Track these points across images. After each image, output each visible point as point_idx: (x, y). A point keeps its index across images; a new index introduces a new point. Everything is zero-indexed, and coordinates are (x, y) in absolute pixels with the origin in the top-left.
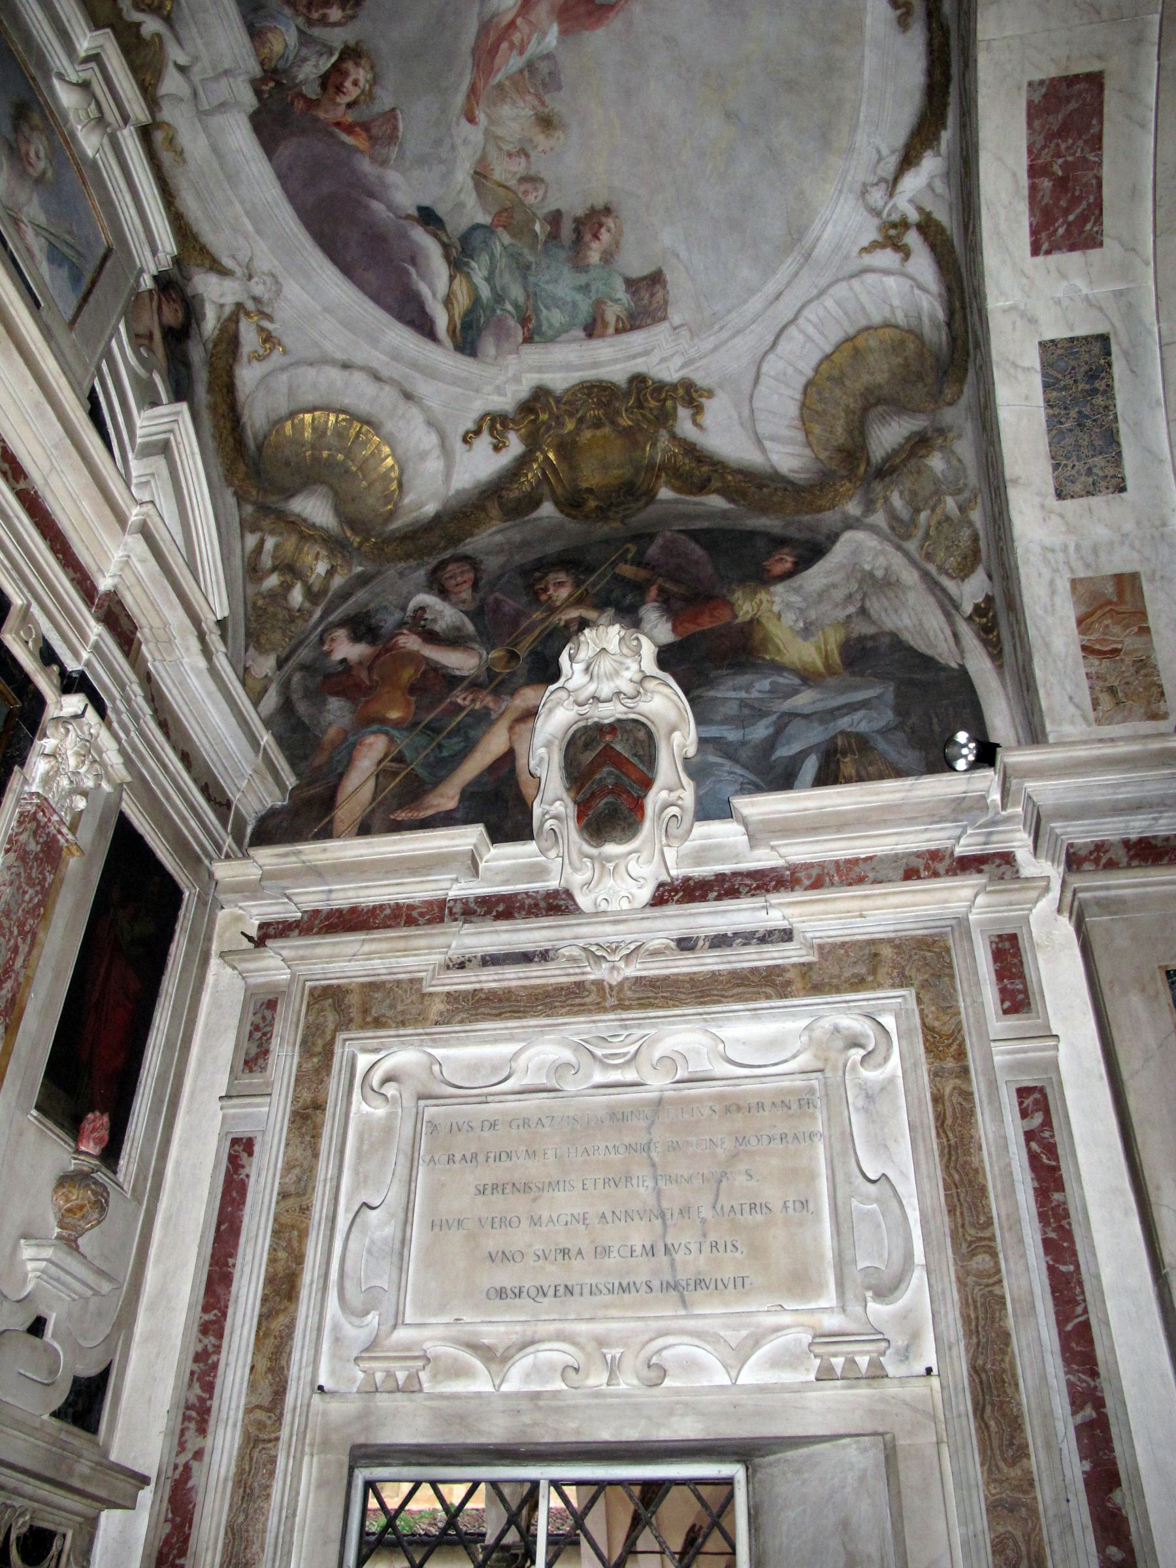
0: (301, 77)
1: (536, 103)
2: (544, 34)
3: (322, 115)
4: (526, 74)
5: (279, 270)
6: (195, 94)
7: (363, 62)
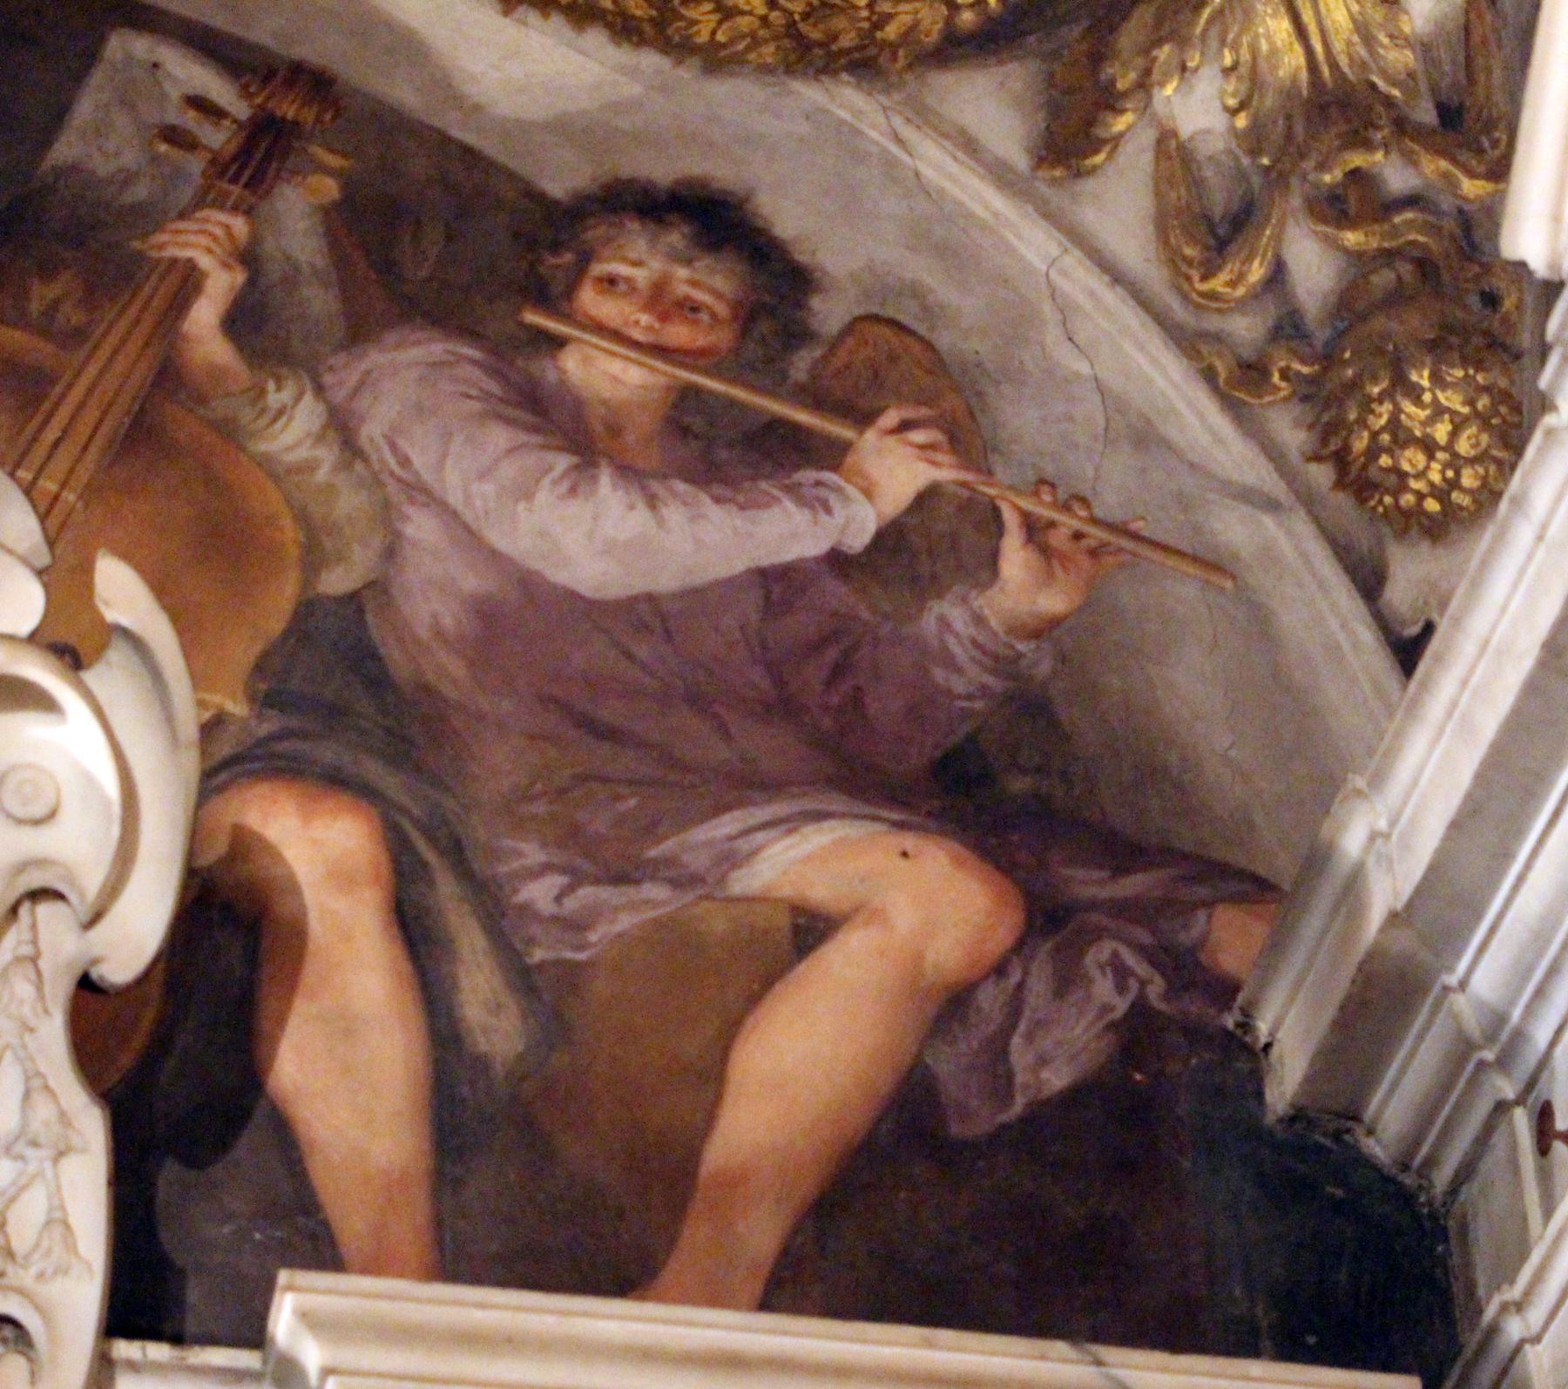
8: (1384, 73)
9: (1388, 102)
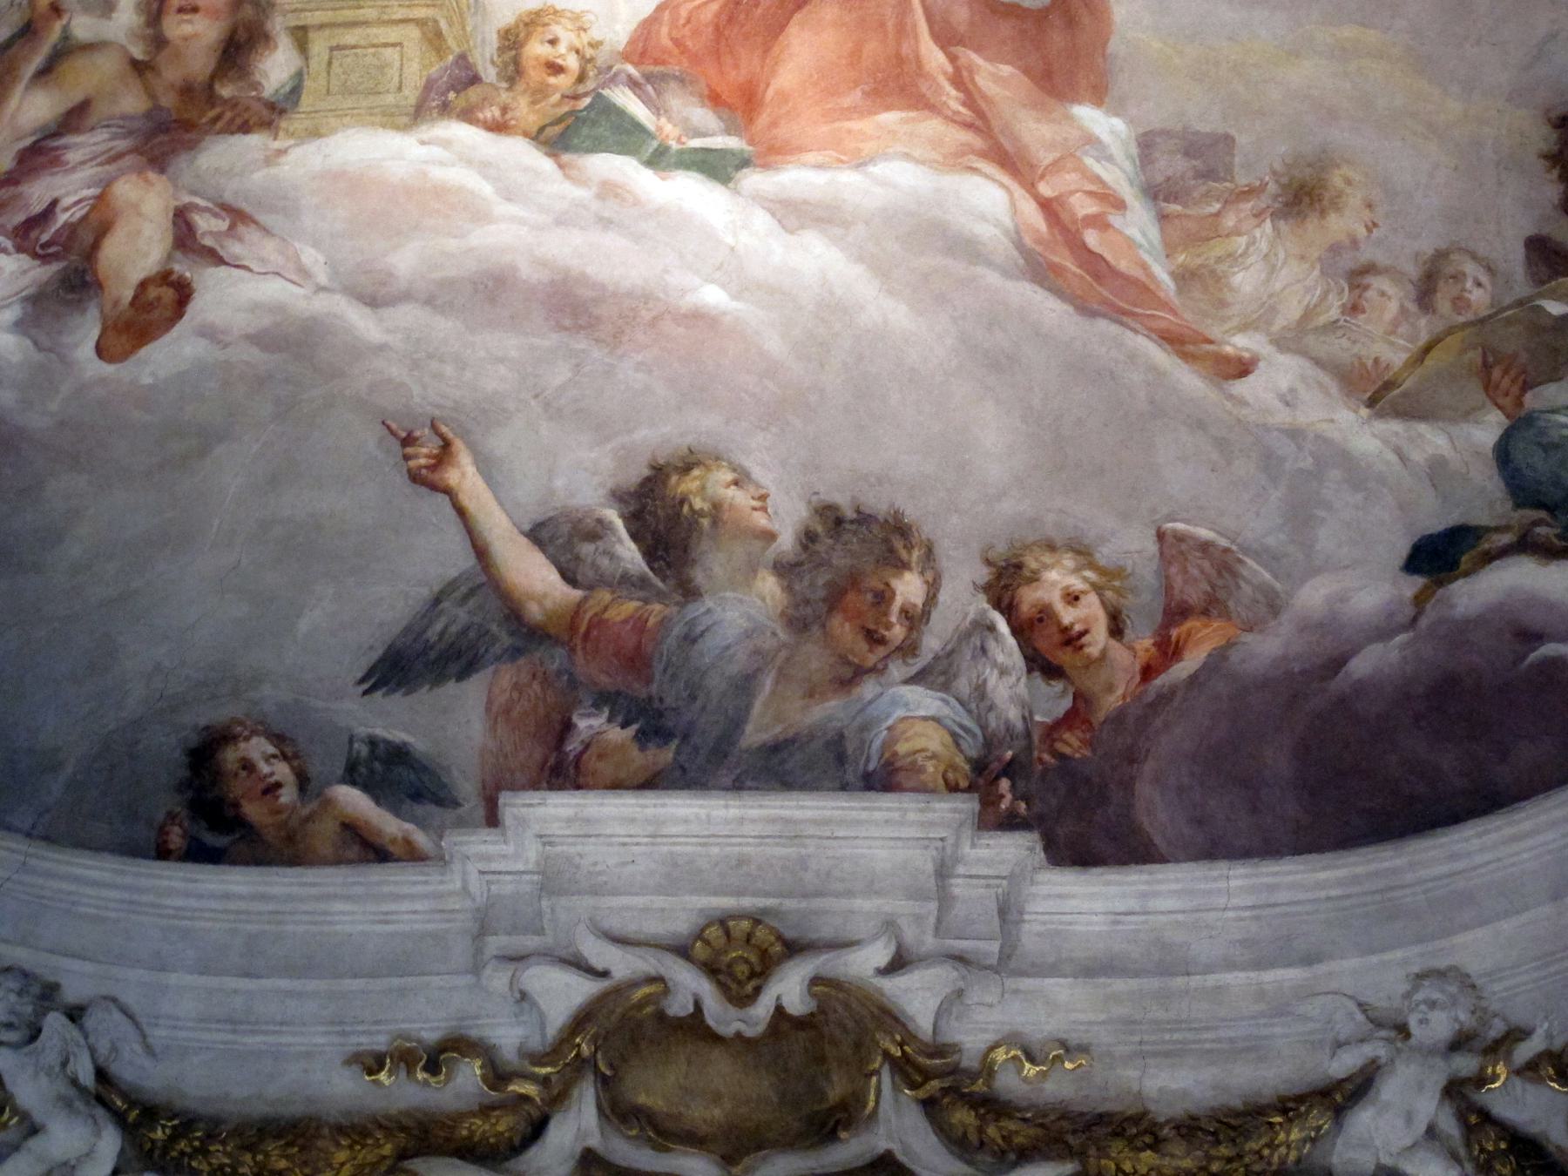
0: (1013, 714)
1: (1247, 206)
2: (1090, 140)
3: (1111, 702)
4: (1175, 208)
5: (1414, 957)
6: (960, 959)
7: (1031, 563)
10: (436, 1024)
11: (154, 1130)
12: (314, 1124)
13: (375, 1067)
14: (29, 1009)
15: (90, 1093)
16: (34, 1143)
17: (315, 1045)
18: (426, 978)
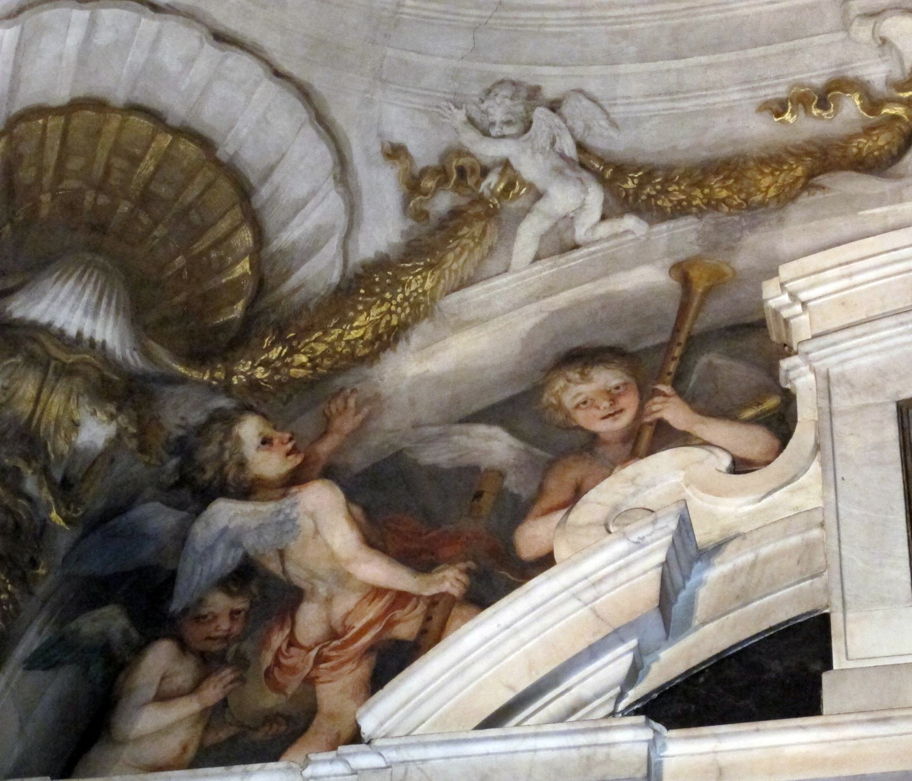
8: (54, 444)
9: (47, 456)
10: (821, 72)
11: (626, 182)
12: (742, 160)
13: (781, 110)
14: (520, 109)
15: (573, 160)
16: (541, 205)
17: (734, 101)
18: (810, 39)
